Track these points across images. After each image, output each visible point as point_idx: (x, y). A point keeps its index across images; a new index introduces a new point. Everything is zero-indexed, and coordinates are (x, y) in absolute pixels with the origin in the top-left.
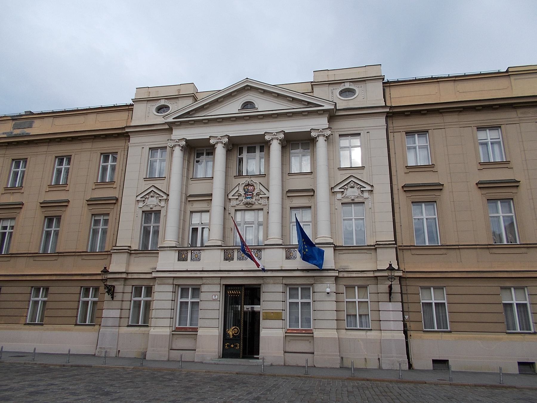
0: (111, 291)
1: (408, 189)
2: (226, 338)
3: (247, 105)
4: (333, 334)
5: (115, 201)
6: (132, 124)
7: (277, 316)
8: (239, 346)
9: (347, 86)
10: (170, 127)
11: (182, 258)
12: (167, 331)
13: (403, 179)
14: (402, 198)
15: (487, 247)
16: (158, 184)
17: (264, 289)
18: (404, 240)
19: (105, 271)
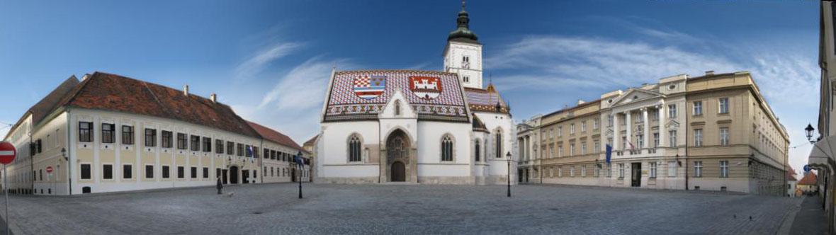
0: (600, 166)
1: (693, 124)
2: (632, 180)
3: (636, 97)
4: (662, 178)
5: (599, 136)
6: (602, 108)
7: (646, 173)
8: (637, 183)
9: (672, 84)
10: (611, 109)
11: (618, 154)
12: (615, 178)
13: (691, 120)
14: (691, 128)
15: (718, 146)
16: (611, 128)
17: (642, 164)
18: (690, 144)
19: (597, 160)
